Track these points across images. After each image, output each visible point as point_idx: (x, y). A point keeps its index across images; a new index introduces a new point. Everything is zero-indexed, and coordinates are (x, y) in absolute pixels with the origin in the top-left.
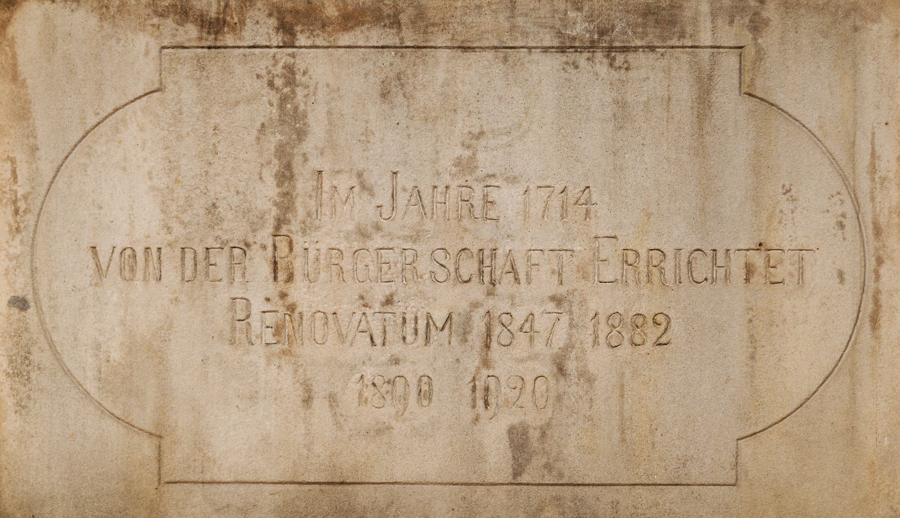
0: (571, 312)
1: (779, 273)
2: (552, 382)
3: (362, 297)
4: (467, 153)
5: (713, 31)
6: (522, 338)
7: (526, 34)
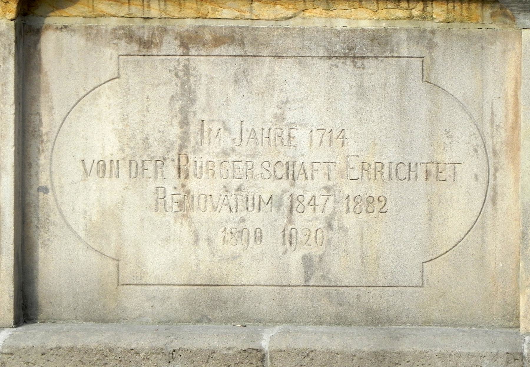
0: (335, 195)
1: (443, 176)
2: (325, 233)
3: (225, 187)
4: (280, 112)
5: (409, 48)
6: (309, 208)
7: (310, 50)
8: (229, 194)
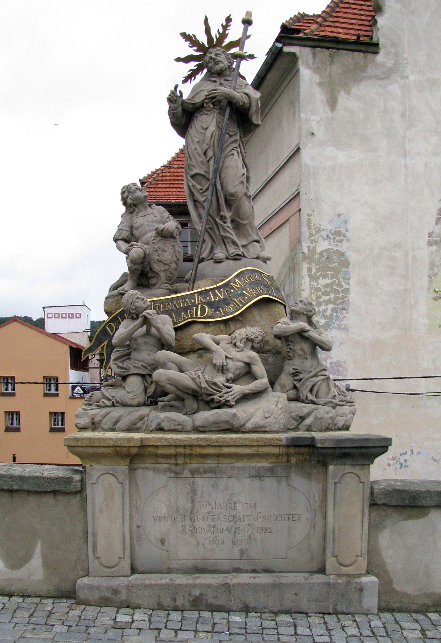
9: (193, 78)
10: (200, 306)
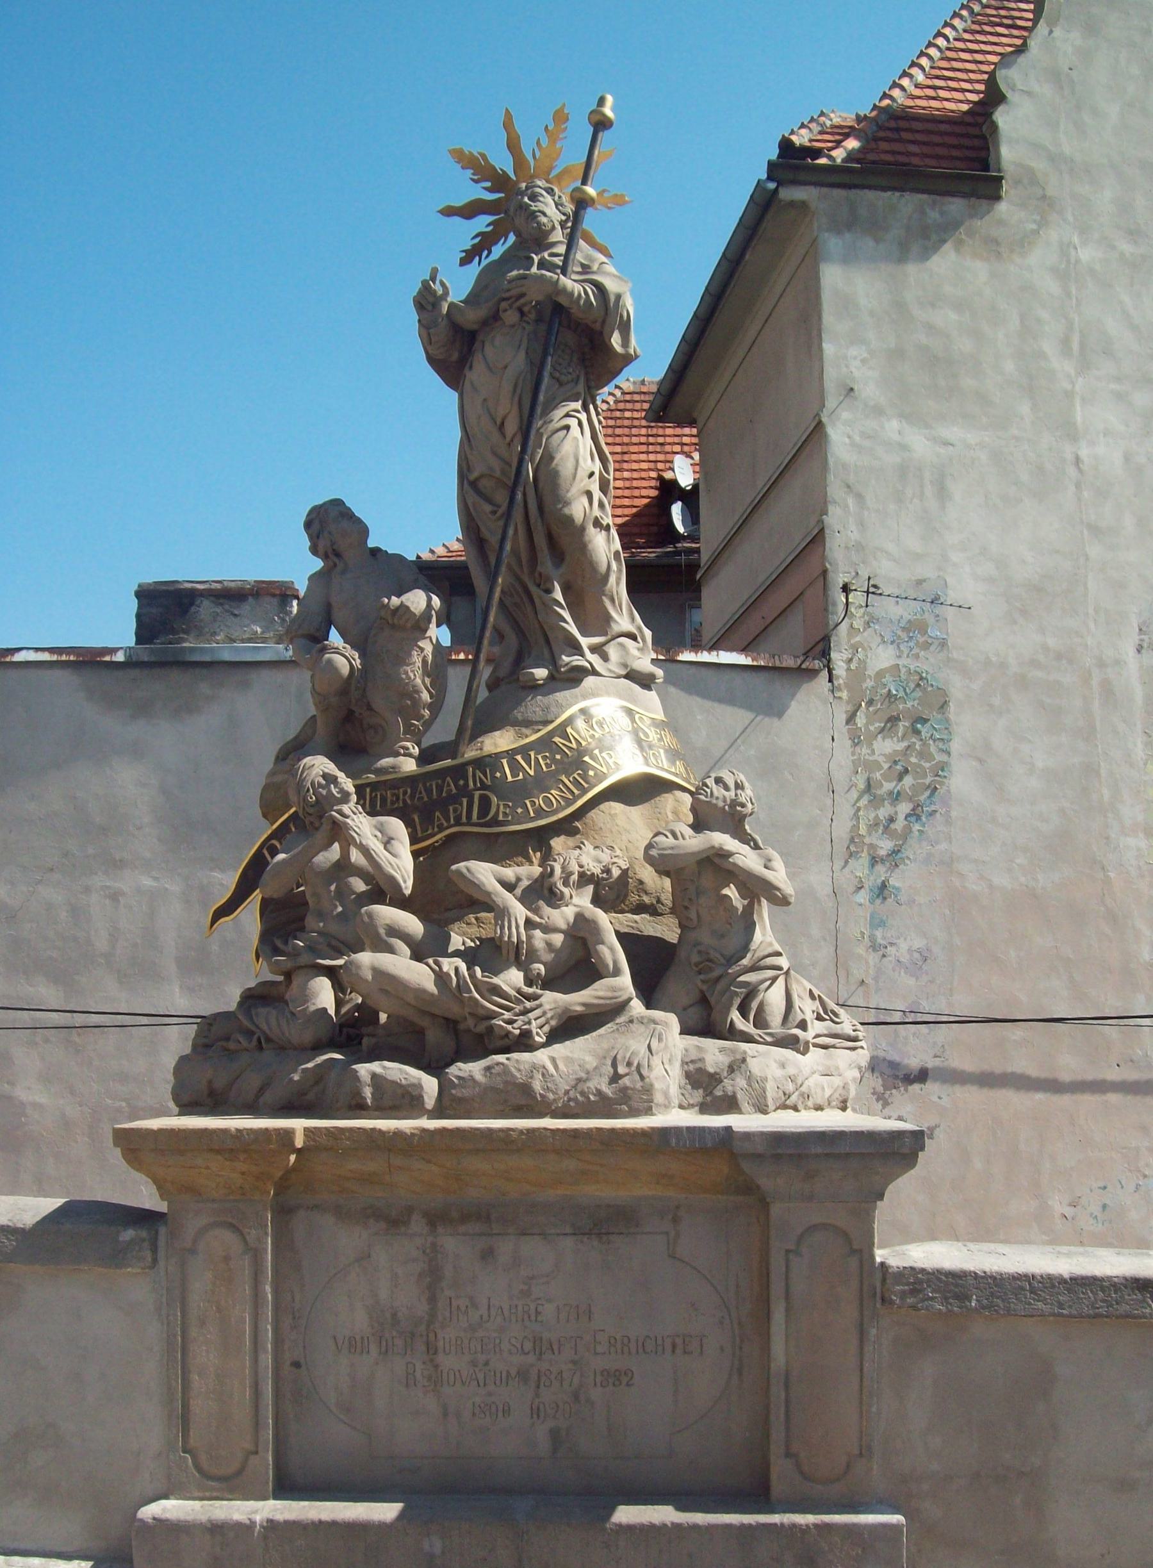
8: (477, 1370)
9: (485, 253)
10: (477, 794)
